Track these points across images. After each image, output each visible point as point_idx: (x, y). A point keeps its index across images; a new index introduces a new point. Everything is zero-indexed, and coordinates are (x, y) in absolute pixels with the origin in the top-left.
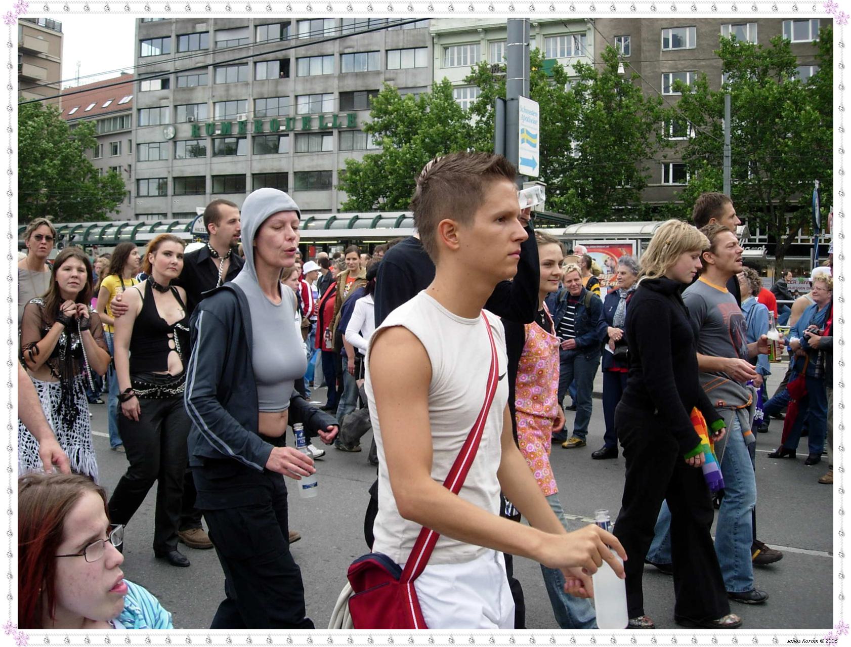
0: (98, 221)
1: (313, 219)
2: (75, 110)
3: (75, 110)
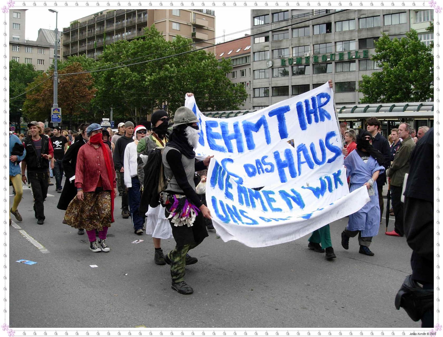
0: (234, 110)
1: (344, 108)
2: (239, 50)
3: (239, 50)
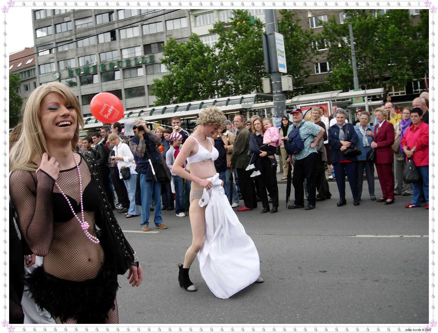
1: (131, 113)
